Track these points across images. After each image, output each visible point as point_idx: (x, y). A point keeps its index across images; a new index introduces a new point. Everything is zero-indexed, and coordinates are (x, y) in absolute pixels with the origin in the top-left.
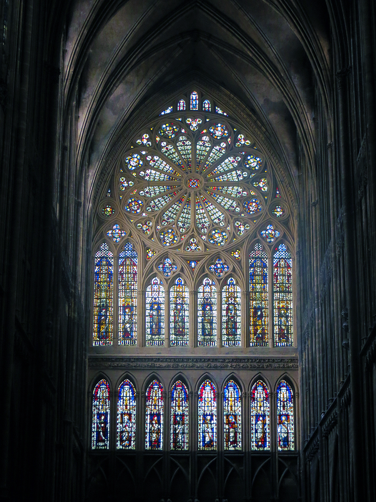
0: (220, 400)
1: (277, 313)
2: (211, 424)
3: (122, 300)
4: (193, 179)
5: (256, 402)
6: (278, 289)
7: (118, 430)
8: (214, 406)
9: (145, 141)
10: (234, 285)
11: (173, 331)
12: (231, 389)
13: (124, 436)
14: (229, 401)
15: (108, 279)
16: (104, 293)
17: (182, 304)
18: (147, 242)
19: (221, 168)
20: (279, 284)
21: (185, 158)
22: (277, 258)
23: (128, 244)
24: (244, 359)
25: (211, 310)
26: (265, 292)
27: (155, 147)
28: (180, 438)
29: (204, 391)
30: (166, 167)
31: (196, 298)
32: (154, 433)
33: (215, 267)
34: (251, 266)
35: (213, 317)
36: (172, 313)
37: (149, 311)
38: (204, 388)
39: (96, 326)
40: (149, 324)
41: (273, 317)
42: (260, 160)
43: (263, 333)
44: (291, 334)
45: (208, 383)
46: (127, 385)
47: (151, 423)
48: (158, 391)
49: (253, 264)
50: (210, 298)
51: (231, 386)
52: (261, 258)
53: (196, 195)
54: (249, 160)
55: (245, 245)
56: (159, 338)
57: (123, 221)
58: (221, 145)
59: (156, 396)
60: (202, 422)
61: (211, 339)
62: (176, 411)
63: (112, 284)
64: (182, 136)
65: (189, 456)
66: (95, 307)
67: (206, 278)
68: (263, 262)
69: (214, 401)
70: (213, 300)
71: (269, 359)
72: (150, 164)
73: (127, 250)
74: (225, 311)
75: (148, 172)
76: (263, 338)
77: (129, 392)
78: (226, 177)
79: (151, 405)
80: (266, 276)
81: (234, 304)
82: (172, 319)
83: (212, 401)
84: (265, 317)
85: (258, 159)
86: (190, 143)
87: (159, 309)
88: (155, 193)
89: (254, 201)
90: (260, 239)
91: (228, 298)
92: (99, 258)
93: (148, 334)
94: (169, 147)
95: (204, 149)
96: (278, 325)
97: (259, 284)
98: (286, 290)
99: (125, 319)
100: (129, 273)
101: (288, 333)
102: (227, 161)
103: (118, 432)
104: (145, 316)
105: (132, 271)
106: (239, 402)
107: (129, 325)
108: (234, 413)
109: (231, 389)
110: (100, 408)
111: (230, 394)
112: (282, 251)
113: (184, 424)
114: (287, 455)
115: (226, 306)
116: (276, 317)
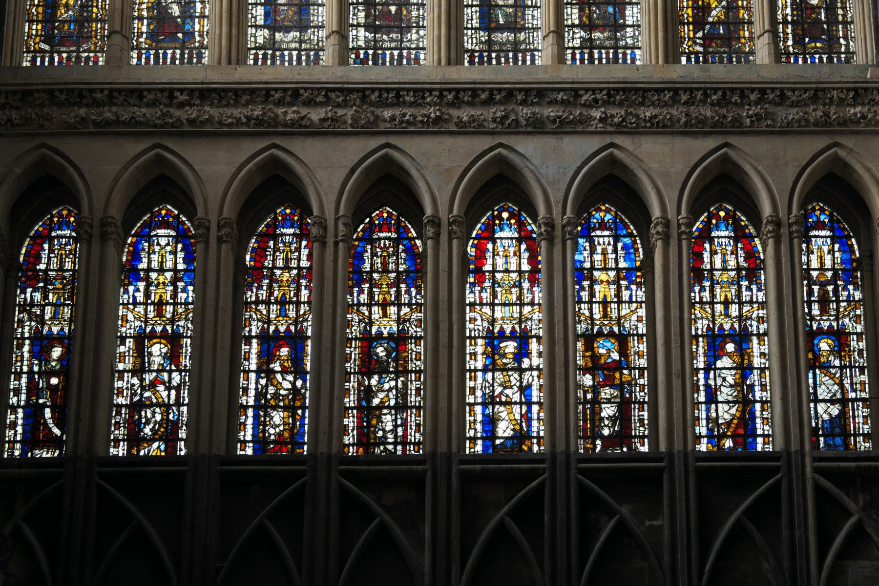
0: (558, 249)
2: (521, 371)
5: (707, 284)
7: (120, 400)
8: (532, 304)
12: (603, 238)
13: (148, 422)
14: (593, 282)
24: (657, 90)
28: (389, 427)
29: (490, 246)
32: (275, 408)
38: (489, 235)
45: (505, 215)
46: (166, 225)
47: (264, 370)
48: (298, 249)
51: (602, 226)
56: (301, 41)
59: (287, 268)
60: (480, 365)
61: (516, 46)
62: (371, 323)
65: (424, 472)
69: (533, 281)
77: (174, 253)
79: (268, 303)
83: (526, 285)
93: (257, 27)
103: (122, 406)
106: (639, 285)
108: (616, 329)
109: (603, 238)
110: (47, 318)
111: (598, 257)
113: (406, 372)
114: (853, 464)
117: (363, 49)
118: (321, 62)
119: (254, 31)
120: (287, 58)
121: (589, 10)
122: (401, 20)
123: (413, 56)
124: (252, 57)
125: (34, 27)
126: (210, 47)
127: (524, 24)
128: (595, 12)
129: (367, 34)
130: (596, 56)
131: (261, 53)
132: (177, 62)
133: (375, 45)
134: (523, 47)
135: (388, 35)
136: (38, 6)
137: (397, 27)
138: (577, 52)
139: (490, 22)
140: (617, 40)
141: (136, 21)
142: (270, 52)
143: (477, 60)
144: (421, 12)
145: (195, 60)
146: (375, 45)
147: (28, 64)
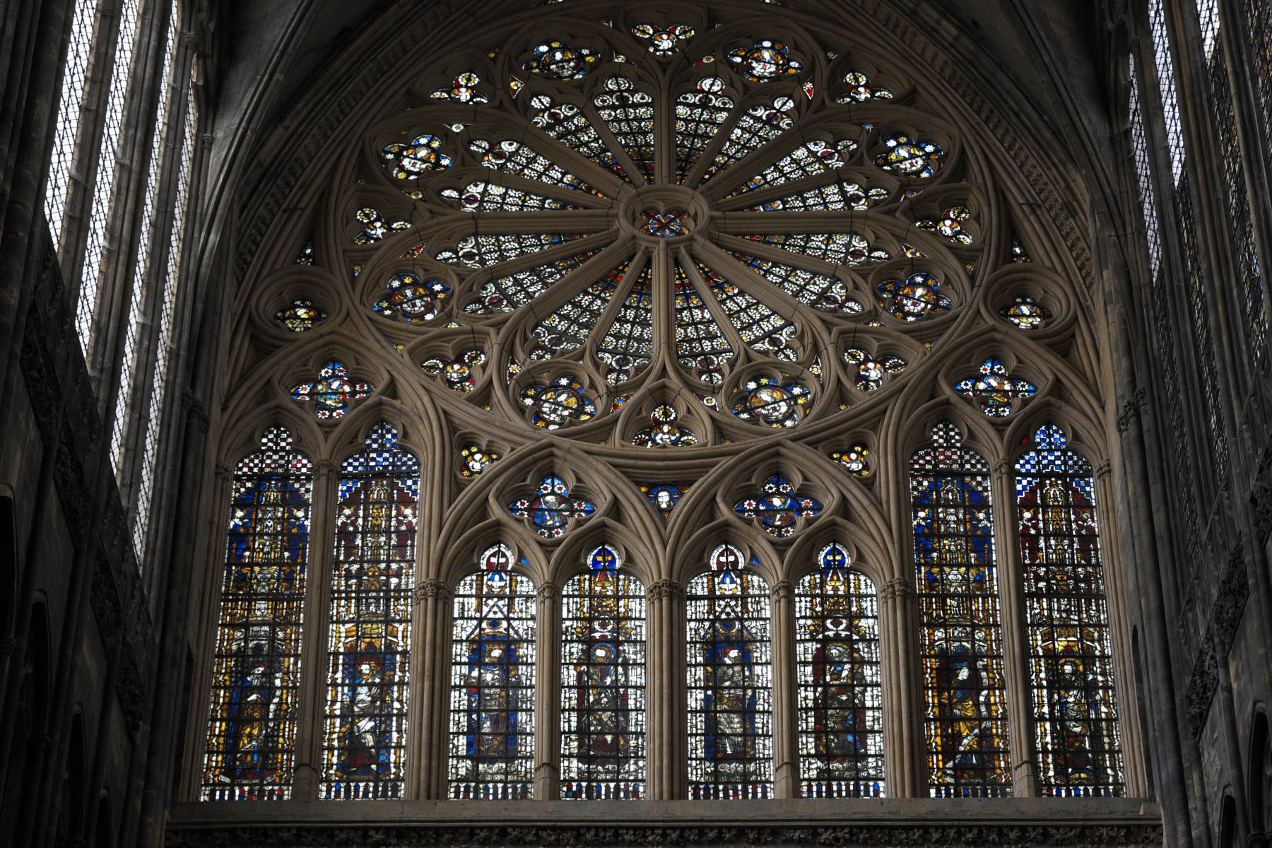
1: (1043, 675)
3: (343, 629)
4: (662, 209)
6: (1042, 584)
9: (464, 95)
10: (847, 572)
11: (575, 744)
15: (286, 554)
16: (262, 605)
17: (617, 643)
18: (468, 416)
19: (776, 175)
20: (1046, 566)
21: (627, 145)
22: (1028, 474)
23: (382, 427)
25: (746, 661)
26: (985, 597)
27: (506, 102)
30: (552, 173)
31: (676, 623)
33: (762, 508)
34: (921, 503)
35: (754, 689)
36: (569, 675)
37: (465, 670)
39: (219, 727)
40: (464, 719)
41: (1028, 688)
42: (936, 152)
43: (987, 750)
44: (1112, 752)
49: (925, 495)
50: (741, 620)
52: (960, 475)
53: (677, 263)
54: (892, 149)
55: (890, 419)
57: (362, 340)
58: (777, 104)
61: (745, 778)
63: (302, 571)
64: (616, 77)
66: (220, 656)
67: (724, 546)
68: (973, 492)
70: (754, 627)
71: (1023, 829)
72: (486, 164)
73: (374, 451)
74: (809, 669)
75: (475, 190)
76: (985, 768)
78: (798, 203)
80: (986, 536)
81: (848, 640)
82: (569, 698)
84: (991, 688)
85: (929, 149)
86: (648, 99)
87: (510, 661)
88: (502, 258)
89: (919, 279)
90: (954, 398)
91: (820, 618)
92: (250, 479)
93: (458, 758)
94: (564, 111)
95: (706, 116)
96: (1052, 719)
97: (959, 566)
98: (1077, 587)
99: (353, 701)
100: (379, 533)
101: (1098, 748)
102: (800, 153)
104: (446, 688)
105: (393, 523)
107: (372, 724)
112: (1051, 451)
115: (812, 646)
116: (1040, 687)
117: (575, 781)
118: (529, 795)
119: (455, 762)
120: (491, 791)
121: (827, 739)
122: (618, 750)
123: (631, 789)
124: (452, 790)
125: (214, 758)
126: (407, 780)
127: (755, 754)
128: (833, 741)
129: (580, 765)
130: (835, 788)
131: (462, 785)
132: (370, 795)
133: (589, 777)
134: (753, 778)
135: (603, 766)
136: (219, 736)
137: (614, 757)
138: (813, 784)
139: (717, 752)
140: (858, 771)
141: (326, 752)
142: (473, 784)
143: (702, 792)
144: (640, 741)
145: (390, 793)
146: (589, 776)
147: (207, 798)
